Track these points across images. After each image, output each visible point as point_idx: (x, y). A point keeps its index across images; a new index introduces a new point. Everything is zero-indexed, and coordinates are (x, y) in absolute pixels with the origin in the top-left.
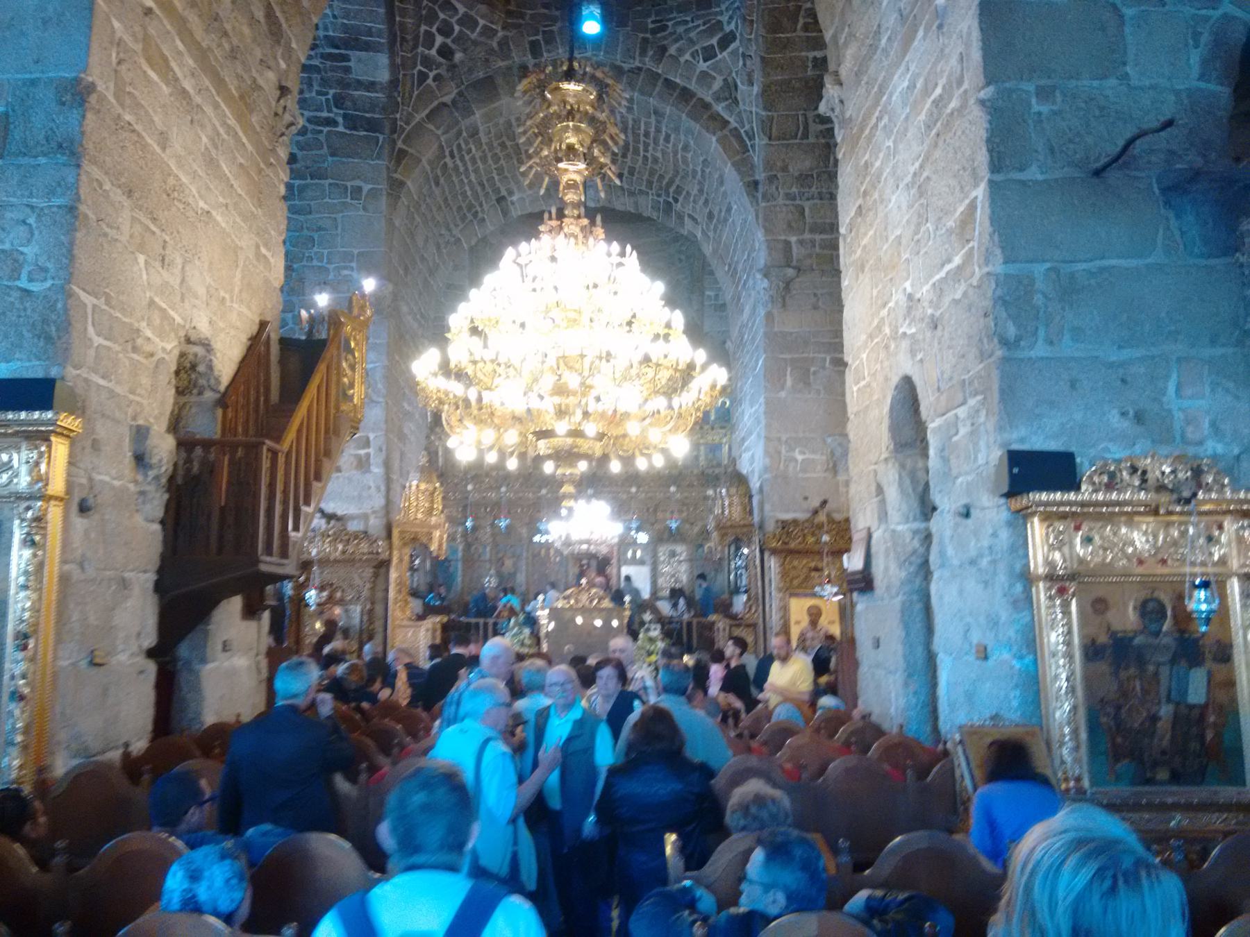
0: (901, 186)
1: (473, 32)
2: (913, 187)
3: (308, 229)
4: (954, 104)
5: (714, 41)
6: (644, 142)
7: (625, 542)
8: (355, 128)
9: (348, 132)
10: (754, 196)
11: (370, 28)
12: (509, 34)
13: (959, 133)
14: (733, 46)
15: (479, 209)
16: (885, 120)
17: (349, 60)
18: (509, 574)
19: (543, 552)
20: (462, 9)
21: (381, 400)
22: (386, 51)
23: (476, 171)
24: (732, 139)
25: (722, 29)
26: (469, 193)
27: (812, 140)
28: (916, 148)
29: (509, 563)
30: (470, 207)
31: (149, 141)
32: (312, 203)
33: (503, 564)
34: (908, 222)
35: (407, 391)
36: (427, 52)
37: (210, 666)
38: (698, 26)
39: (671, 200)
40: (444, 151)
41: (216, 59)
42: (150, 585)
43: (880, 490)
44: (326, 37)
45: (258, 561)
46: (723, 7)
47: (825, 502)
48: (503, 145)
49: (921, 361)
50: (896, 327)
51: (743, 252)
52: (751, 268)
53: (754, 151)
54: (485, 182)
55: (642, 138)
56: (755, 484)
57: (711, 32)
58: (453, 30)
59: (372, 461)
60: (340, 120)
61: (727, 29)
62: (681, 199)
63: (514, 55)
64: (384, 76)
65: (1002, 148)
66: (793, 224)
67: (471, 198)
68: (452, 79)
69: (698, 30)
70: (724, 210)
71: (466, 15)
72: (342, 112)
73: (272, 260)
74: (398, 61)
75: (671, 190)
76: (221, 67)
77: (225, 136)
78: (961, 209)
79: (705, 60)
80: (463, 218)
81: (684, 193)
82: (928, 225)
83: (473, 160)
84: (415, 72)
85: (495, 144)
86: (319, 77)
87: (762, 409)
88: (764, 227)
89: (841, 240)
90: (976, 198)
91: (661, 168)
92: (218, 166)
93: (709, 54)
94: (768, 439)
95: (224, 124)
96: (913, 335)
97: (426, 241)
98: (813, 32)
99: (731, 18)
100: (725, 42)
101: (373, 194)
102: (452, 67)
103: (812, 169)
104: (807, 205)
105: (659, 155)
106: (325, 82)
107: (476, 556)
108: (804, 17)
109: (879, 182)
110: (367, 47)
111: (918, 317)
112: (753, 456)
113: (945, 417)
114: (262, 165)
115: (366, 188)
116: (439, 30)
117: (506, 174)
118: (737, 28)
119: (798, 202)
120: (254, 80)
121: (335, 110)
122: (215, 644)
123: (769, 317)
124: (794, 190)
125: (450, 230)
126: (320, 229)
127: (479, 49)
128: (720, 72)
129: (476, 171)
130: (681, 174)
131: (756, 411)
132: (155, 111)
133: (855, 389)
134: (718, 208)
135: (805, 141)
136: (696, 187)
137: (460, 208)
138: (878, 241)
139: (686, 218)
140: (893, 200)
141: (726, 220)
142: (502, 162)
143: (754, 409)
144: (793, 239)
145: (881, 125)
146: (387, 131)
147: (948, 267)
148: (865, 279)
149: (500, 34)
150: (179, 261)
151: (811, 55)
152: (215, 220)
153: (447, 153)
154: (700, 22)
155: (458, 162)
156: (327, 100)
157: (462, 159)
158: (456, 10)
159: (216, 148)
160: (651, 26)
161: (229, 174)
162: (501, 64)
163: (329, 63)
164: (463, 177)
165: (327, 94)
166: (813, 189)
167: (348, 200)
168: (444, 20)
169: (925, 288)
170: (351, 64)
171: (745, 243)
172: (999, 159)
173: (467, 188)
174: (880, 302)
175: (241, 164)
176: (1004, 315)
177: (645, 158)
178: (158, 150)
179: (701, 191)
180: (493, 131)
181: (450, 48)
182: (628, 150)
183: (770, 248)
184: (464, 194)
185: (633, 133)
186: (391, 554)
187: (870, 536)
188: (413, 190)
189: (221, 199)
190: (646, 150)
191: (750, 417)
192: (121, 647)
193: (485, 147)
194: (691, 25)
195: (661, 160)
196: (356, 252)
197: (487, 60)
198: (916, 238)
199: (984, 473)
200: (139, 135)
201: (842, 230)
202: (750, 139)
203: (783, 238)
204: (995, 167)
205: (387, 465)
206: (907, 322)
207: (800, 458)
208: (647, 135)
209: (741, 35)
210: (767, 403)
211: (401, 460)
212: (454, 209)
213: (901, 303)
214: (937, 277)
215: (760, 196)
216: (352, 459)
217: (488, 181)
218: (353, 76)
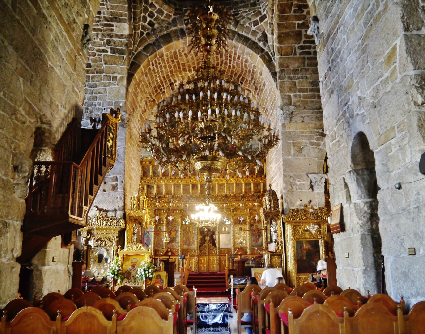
0: (351, 53)
1: (162, 16)
2: (358, 51)
3: (95, 93)
4: (381, 8)
5: (258, 18)
6: (229, 60)
7: (222, 223)
8: (114, 53)
9: (112, 55)
10: (275, 78)
11: (121, 13)
12: (176, 17)
13: (383, 21)
14: (265, 20)
15: (162, 87)
16: (342, 27)
17: (113, 26)
18: (173, 238)
19: (187, 228)
20: (158, 7)
21: (123, 161)
22: (128, 22)
23: (162, 72)
24: (266, 56)
25: (261, 14)
26: (159, 81)
27: (298, 55)
28: (359, 34)
29: (173, 233)
30: (159, 86)
31: (27, 30)
32: (97, 83)
33: (171, 234)
34: (357, 66)
35: (133, 159)
36: (144, 24)
37: (46, 268)
38: (251, 13)
39: (240, 83)
40: (150, 63)
41: (58, 5)
42: (19, 228)
43: (346, 186)
44: (104, 17)
45: (68, 217)
46: (261, 6)
47: (310, 202)
48: (173, 61)
49: (368, 123)
50: (353, 112)
51: (271, 101)
52: (274, 107)
53: (275, 60)
54: (165, 77)
55: (229, 58)
56: (279, 196)
57: (256, 15)
58: (154, 15)
59: (118, 187)
60: (109, 50)
61: (263, 14)
62: (244, 83)
63: (178, 25)
64: (126, 32)
65: (408, 21)
66: (292, 89)
67: (159, 83)
68: (154, 34)
69: (251, 14)
70: (262, 85)
71: (159, 9)
72: (109, 47)
73: (79, 94)
74: (133, 27)
75: (240, 79)
76: (60, 9)
77: (61, 38)
78: (386, 53)
79: (254, 26)
80: (156, 91)
81: (245, 80)
82: (369, 64)
83: (161, 67)
84: (139, 31)
85: (170, 61)
86: (101, 33)
87: (282, 163)
88: (280, 90)
89: (320, 84)
90: (396, 44)
91: (236, 70)
92: (57, 49)
94: (285, 176)
95: (61, 32)
96: (362, 114)
97: (142, 99)
98: (297, 13)
99: (264, 9)
100: (263, 18)
101: (122, 78)
102: (154, 30)
103: (298, 67)
104: (297, 81)
105: (235, 65)
106: (103, 35)
108: (294, 7)
109: (340, 54)
110: (120, 21)
111: (365, 105)
112: (277, 184)
113: (384, 145)
114: (77, 54)
115: (119, 76)
117: (174, 73)
118: (267, 13)
119: (293, 80)
120: (74, 19)
121: (107, 46)
122: (49, 258)
123: (284, 125)
124: (292, 75)
125: (151, 96)
126: (99, 93)
127: (164, 23)
128: (260, 31)
129: (162, 72)
130: (244, 72)
131: (279, 165)
132: (30, 18)
133: (331, 144)
134: (259, 85)
135: (295, 56)
136: (251, 77)
137: (155, 87)
138: (341, 78)
139: (246, 91)
140: (348, 59)
141: (263, 90)
142: (172, 68)
143: (277, 164)
144: (292, 95)
145: (339, 31)
146: (127, 54)
147: (381, 79)
148: (335, 96)
149: (173, 17)
150: (38, 84)
151: (297, 22)
152: (55, 71)
153: (151, 64)
154: (252, 11)
155: (155, 68)
156: (104, 42)
157: (157, 66)
158: (155, 7)
159: (57, 41)
160: (233, 13)
161: (62, 54)
162: (173, 28)
163: (105, 28)
164: (157, 74)
165: (104, 40)
166: (299, 75)
167: (111, 81)
168: (151, 11)
169: (368, 92)
170: (114, 28)
171: (271, 98)
172: (407, 25)
173: (158, 79)
174: (343, 104)
175: (67, 51)
176: (416, 92)
177: (230, 66)
178: (31, 35)
179: (252, 79)
180: (169, 55)
181: (153, 22)
182: (223, 63)
183: (283, 98)
184: (157, 81)
185: (225, 56)
186: (126, 226)
187: (342, 208)
188: (137, 78)
189: (58, 63)
190: (230, 63)
191: (275, 167)
192: (3, 255)
193: (166, 62)
194: (248, 13)
195: (236, 67)
196: (113, 101)
197: (168, 27)
198: (362, 71)
199: (409, 167)
200: (22, 26)
201: (321, 79)
202: (273, 56)
203: (288, 94)
204: (407, 29)
205: (124, 189)
206: (359, 109)
207: (298, 183)
208: (230, 56)
209: (269, 15)
210: (283, 161)
211: (130, 187)
212: (153, 87)
213: (355, 101)
214: (375, 85)
215: (278, 77)
216: (110, 186)
217: (167, 76)
218: (115, 32)
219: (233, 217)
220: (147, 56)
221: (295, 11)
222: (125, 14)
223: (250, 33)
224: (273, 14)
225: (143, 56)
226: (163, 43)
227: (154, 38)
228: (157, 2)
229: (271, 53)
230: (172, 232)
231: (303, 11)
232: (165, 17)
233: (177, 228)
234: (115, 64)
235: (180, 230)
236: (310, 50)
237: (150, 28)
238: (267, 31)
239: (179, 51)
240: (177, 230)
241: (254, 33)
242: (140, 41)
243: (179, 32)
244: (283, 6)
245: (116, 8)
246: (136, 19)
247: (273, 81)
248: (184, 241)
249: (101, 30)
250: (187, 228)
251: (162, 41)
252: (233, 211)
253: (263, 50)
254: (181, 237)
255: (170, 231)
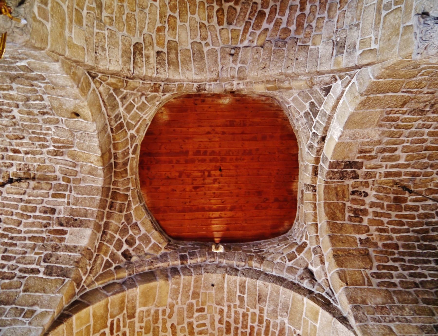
1: (147, 245)
5: (294, 250)
12: (168, 252)
14: (306, 249)
20: (143, 231)
36: (115, 251)
57: (291, 246)
68: (127, 268)
69: (282, 248)
79: (290, 260)
93: (291, 257)
98: (355, 222)
110: (81, 224)
116: (127, 241)
127: (148, 256)
128: (300, 266)
149: (163, 251)
151: (358, 236)
153: (109, 324)
160: (253, 251)
165: (42, 253)
170: (66, 236)
202: (331, 297)
220: (107, 296)
221: (350, 218)
222: (93, 211)
223: (285, 271)
224: (317, 232)
225: (99, 295)
226: (138, 281)
227: (125, 274)
228: (143, 224)
229: (327, 293)
231: (361, 220)
232: (152, 248)
234: (44, 291)
236: (393, 281)
237: (124, 260)
238: (311, 264)
239: (164, 312)
241: (291, 270)
242: (101, 275)
243: (169, 271)
244: (333, 208)
245: (81, 202)
246: (106, 234)
247: (347, 329)
249: (43, 239)
251: (139, 279)
253: (311, 292)
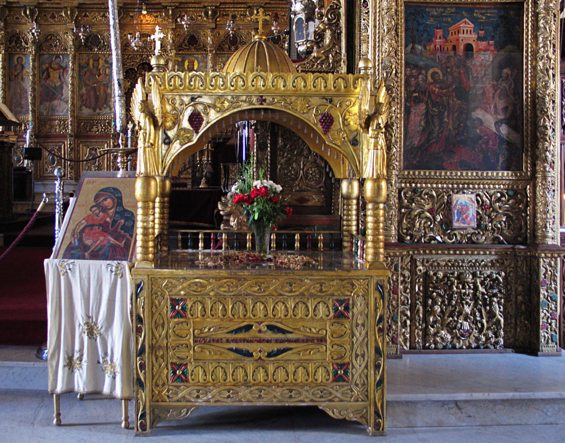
18: (55, 88)
19: (91, 62)
29: (54, 75)
33: (48, 76)
107: (19, 67)
219: (213, 30)
230: (51, 70)
233: (65, 60)
235: (71, 65)
240: (64, 65)
248: (82, 96)
250: (91, 62)
252: (214, 13)
254: (72, 84)
255: (47, 69)
